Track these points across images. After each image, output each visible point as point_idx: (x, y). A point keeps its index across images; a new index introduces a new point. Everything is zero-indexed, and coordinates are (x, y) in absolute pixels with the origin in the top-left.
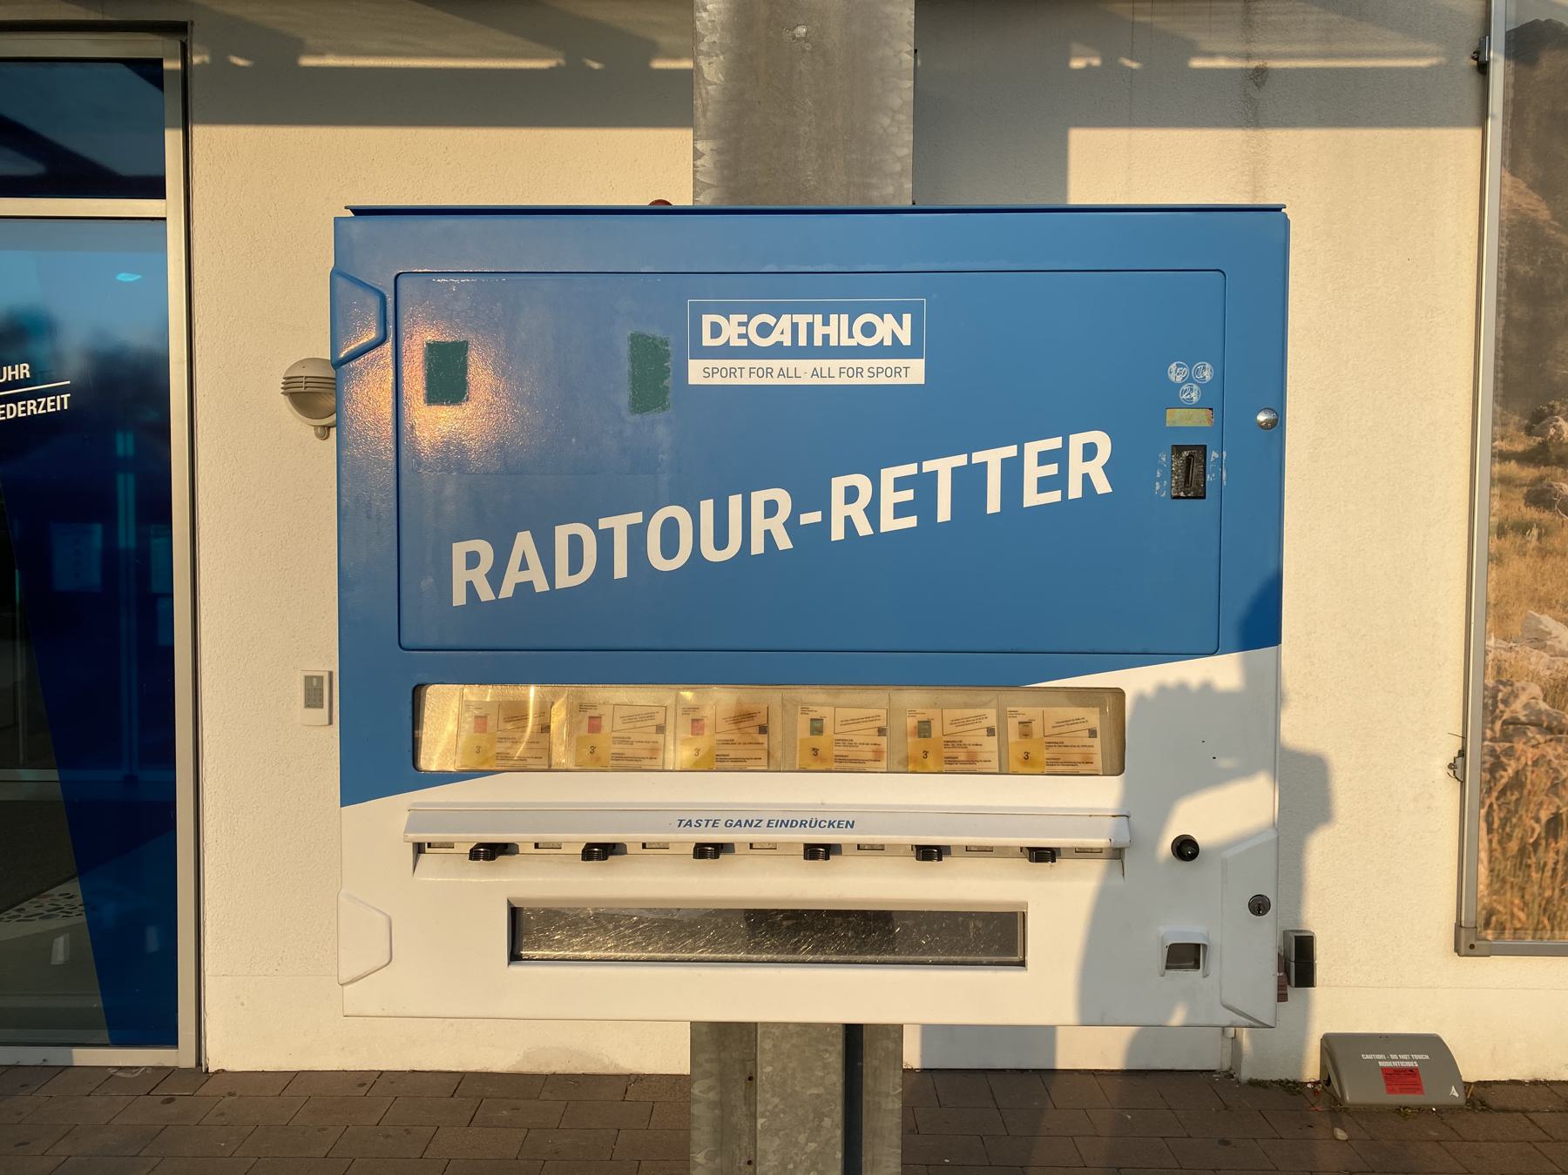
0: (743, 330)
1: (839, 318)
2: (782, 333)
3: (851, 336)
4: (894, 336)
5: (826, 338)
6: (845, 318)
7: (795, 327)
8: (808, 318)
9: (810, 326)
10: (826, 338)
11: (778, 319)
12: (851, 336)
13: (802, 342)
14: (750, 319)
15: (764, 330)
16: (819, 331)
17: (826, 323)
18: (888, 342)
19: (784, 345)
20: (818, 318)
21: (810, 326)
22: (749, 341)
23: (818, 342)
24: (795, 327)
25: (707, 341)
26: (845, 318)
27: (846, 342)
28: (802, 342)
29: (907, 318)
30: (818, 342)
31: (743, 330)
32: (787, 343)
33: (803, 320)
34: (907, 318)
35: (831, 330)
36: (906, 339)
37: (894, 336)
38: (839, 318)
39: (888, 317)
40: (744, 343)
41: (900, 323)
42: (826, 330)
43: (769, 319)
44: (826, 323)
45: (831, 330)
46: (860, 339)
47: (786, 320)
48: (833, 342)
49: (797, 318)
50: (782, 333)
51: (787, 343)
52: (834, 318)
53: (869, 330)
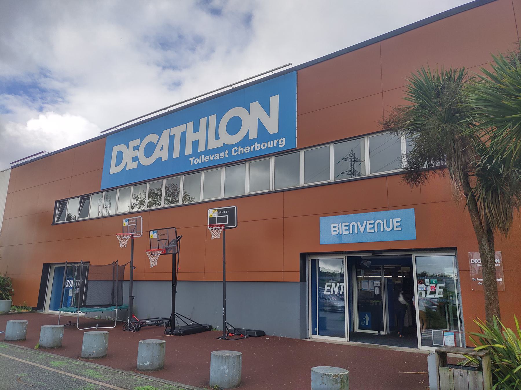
0: (135, 154)
2: (162, 149)
3: (217, 137)
4: (261, 126)
8: (182, 128)
12: (217, 137)
13: (176, 154)
15: (150, 149)
17: (196, 129)
18: (253, 135)
22: (139, 164)
25: (114, 169)
28: (176, 154)
29: (274, 101)
32: (165, 158)
35: (200, 136)
37: (261, 126)
39: (255, 106)
40: (135, 165)
41: (267, 109)
44: (196, 129)
48: (202, 148)
50: (162, 149)
51: (165, 158)
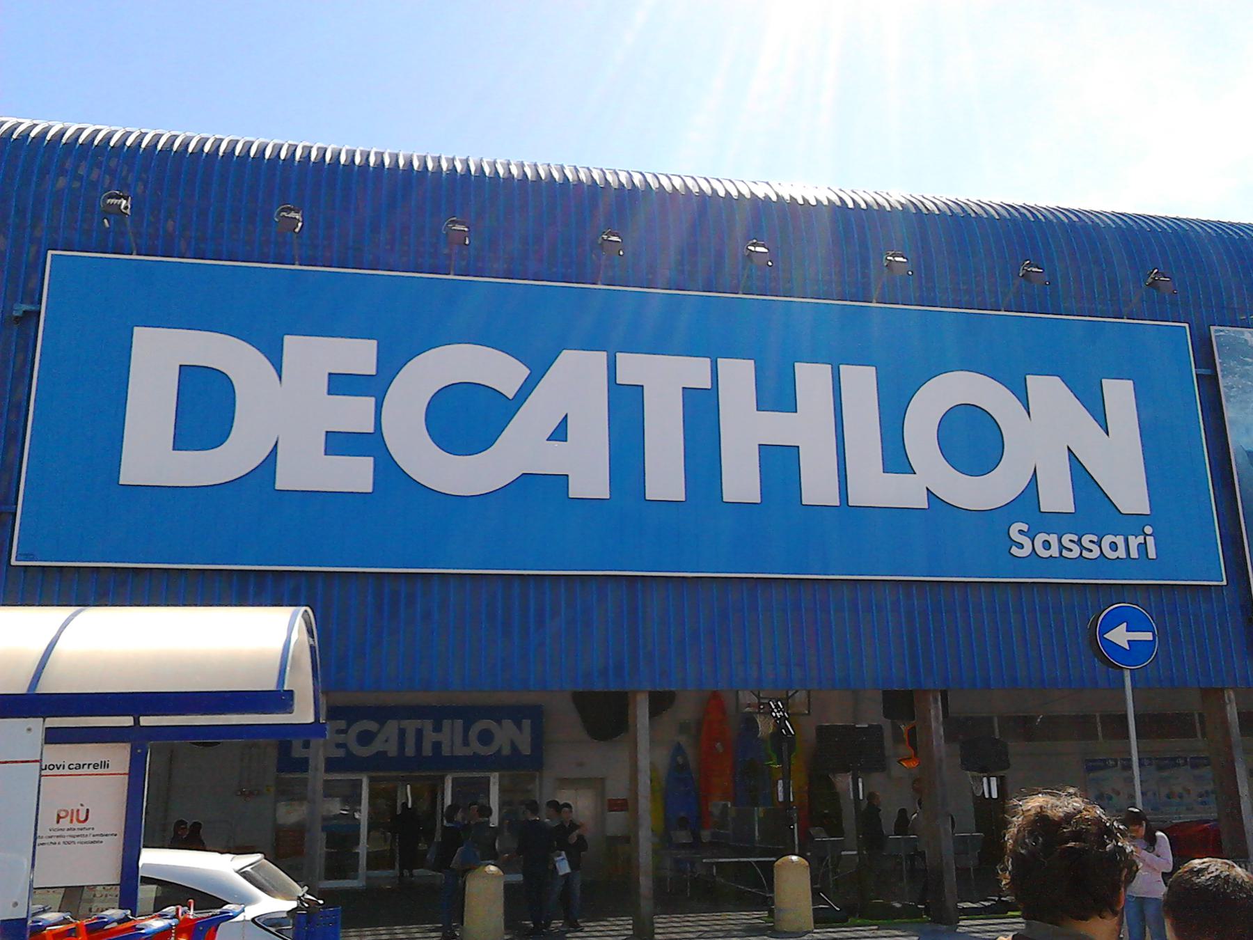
0: (341, 738)
1: (453, 723)
3: (466, 742)
4: (513, 744)
5: (437, 746)
6: (459, 723)
7: (402, 733)
8: (417, 723)
9: (419, 733)
10: (437, 746)
11: (382, 724)
12: (466, 742)
13: (410, 751)
14: (349, 726)
15: (366, 738)
16: (430, 737)
17: (438, 728)
18: (506, 751)
19: (390, 755)
20: (428, 725)
21: (419, 733)
23: (427, 750)
24: (402, 733)
26: (459, 723)
27: (460, 751)
28: (410, 751)
30: (427, 750)
31: (341, 738)
33: (411, 725)
34: (527, 723)
35: (444, 737)
36: (526, 750)
37: (513, 744)
38: (453, 723)
39: (508, 723)
40: (340, 753)
42: (435, 737)
43: (371, 726)
44: (438, 728)
45: (444, 737)
46: (476, 747)
47: (392, 727)
48: (446, 751)
49: (406, 723)
51: (393, 750)
52: (447, 723)
53: (486, 738)
